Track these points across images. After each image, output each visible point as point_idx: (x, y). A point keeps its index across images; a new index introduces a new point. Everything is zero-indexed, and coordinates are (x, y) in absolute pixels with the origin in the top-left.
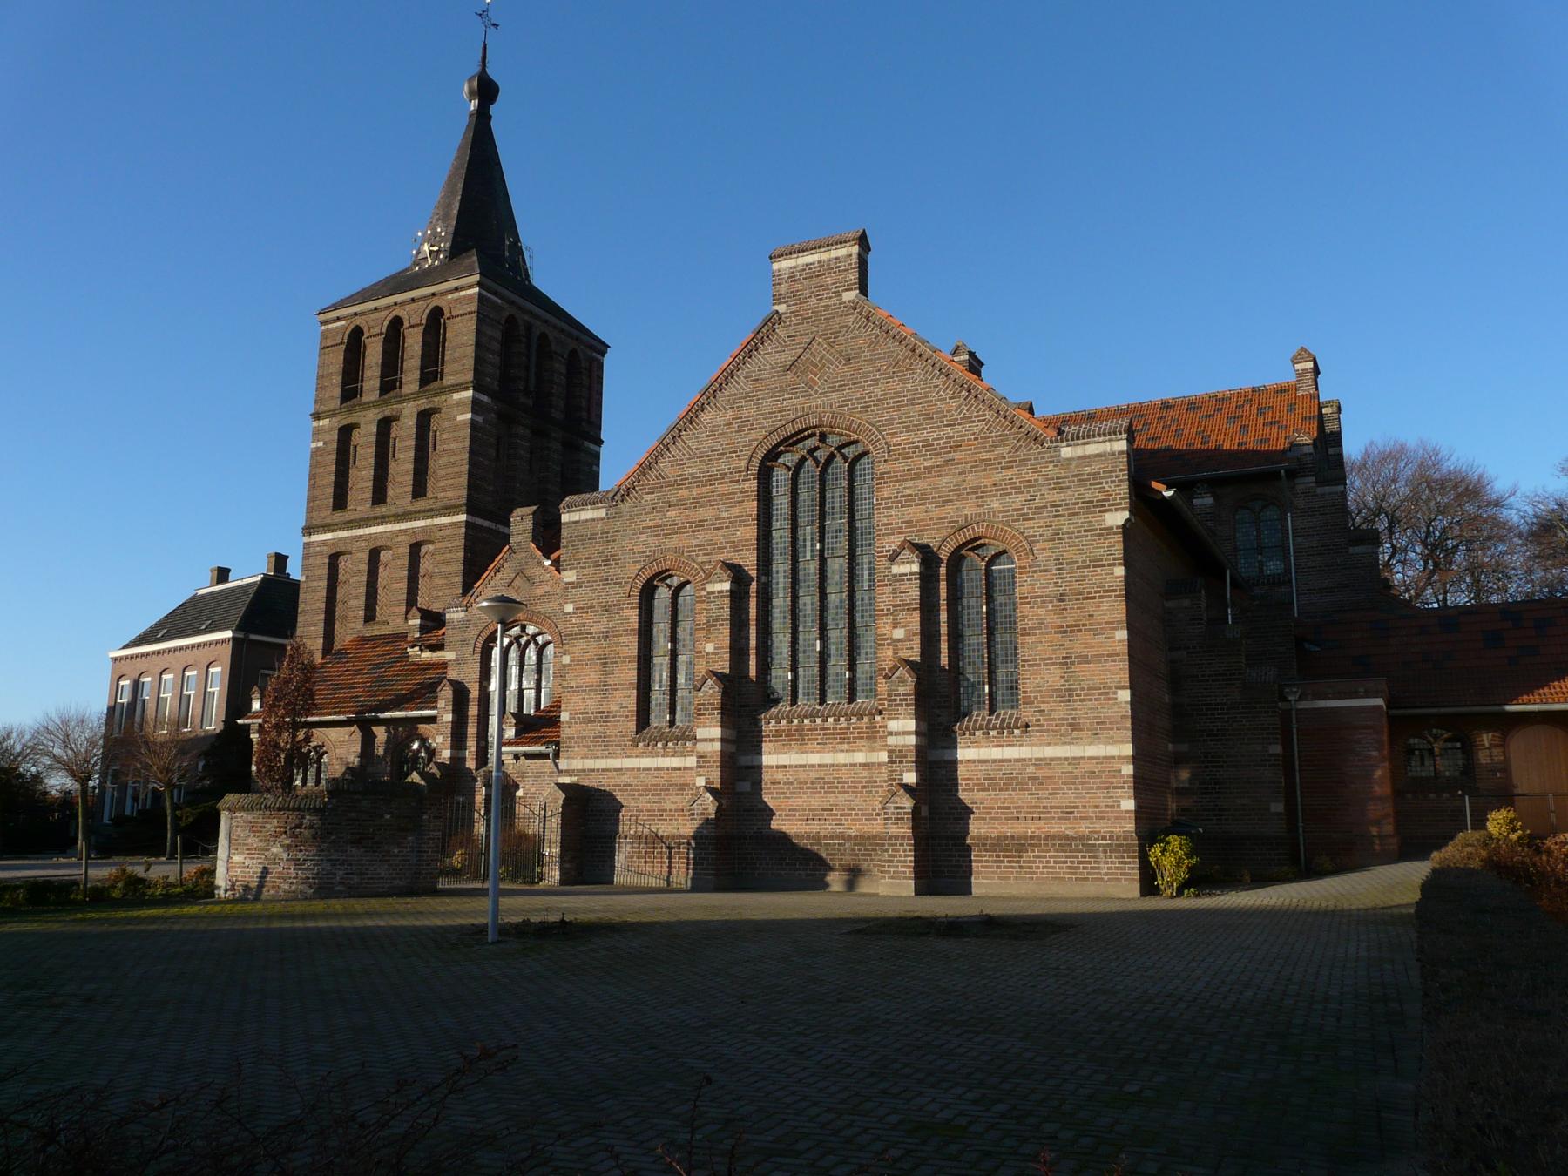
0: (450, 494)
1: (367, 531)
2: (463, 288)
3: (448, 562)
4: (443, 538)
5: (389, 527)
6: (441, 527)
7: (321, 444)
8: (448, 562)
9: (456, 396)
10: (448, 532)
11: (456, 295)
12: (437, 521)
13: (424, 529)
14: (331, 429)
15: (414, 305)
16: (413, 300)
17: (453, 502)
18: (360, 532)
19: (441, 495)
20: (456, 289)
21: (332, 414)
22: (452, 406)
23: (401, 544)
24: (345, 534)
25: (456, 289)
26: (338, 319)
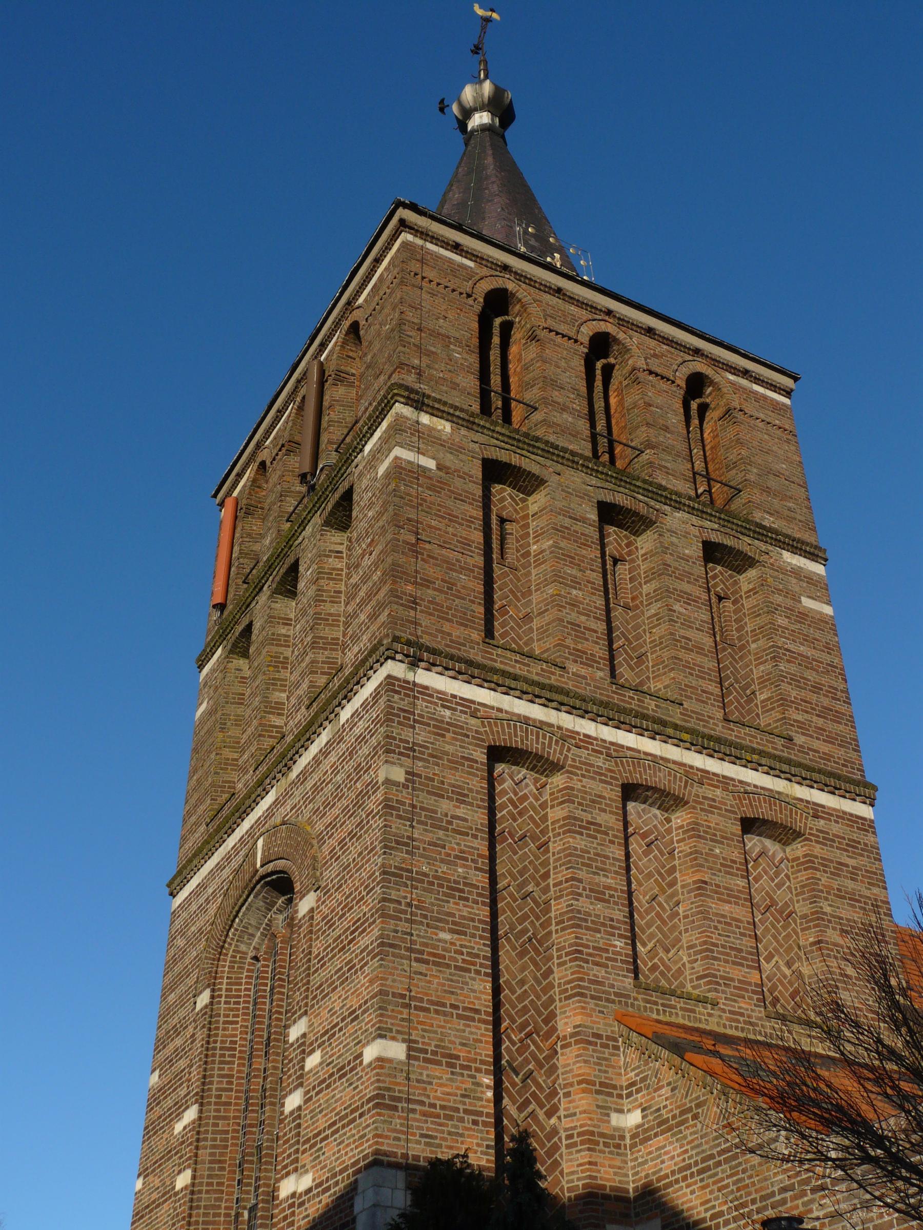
0: (825, 748)
2: (758, 380)
4: (826, 839)
5: (672, 752)
6: (818, 811)
7: (431, 464)
9: (787, 556)
10: (836, 828)
11: (744, 382)
12: (802, 792)
13: (773, 796)
14: (456, 449)
16: (650, 331)
17: (830, 767)
19: (800, 739)
20: (745, 373)
23: (713, 806)
24: (536, 712)
25: (745, 373)
26: (456, 247)
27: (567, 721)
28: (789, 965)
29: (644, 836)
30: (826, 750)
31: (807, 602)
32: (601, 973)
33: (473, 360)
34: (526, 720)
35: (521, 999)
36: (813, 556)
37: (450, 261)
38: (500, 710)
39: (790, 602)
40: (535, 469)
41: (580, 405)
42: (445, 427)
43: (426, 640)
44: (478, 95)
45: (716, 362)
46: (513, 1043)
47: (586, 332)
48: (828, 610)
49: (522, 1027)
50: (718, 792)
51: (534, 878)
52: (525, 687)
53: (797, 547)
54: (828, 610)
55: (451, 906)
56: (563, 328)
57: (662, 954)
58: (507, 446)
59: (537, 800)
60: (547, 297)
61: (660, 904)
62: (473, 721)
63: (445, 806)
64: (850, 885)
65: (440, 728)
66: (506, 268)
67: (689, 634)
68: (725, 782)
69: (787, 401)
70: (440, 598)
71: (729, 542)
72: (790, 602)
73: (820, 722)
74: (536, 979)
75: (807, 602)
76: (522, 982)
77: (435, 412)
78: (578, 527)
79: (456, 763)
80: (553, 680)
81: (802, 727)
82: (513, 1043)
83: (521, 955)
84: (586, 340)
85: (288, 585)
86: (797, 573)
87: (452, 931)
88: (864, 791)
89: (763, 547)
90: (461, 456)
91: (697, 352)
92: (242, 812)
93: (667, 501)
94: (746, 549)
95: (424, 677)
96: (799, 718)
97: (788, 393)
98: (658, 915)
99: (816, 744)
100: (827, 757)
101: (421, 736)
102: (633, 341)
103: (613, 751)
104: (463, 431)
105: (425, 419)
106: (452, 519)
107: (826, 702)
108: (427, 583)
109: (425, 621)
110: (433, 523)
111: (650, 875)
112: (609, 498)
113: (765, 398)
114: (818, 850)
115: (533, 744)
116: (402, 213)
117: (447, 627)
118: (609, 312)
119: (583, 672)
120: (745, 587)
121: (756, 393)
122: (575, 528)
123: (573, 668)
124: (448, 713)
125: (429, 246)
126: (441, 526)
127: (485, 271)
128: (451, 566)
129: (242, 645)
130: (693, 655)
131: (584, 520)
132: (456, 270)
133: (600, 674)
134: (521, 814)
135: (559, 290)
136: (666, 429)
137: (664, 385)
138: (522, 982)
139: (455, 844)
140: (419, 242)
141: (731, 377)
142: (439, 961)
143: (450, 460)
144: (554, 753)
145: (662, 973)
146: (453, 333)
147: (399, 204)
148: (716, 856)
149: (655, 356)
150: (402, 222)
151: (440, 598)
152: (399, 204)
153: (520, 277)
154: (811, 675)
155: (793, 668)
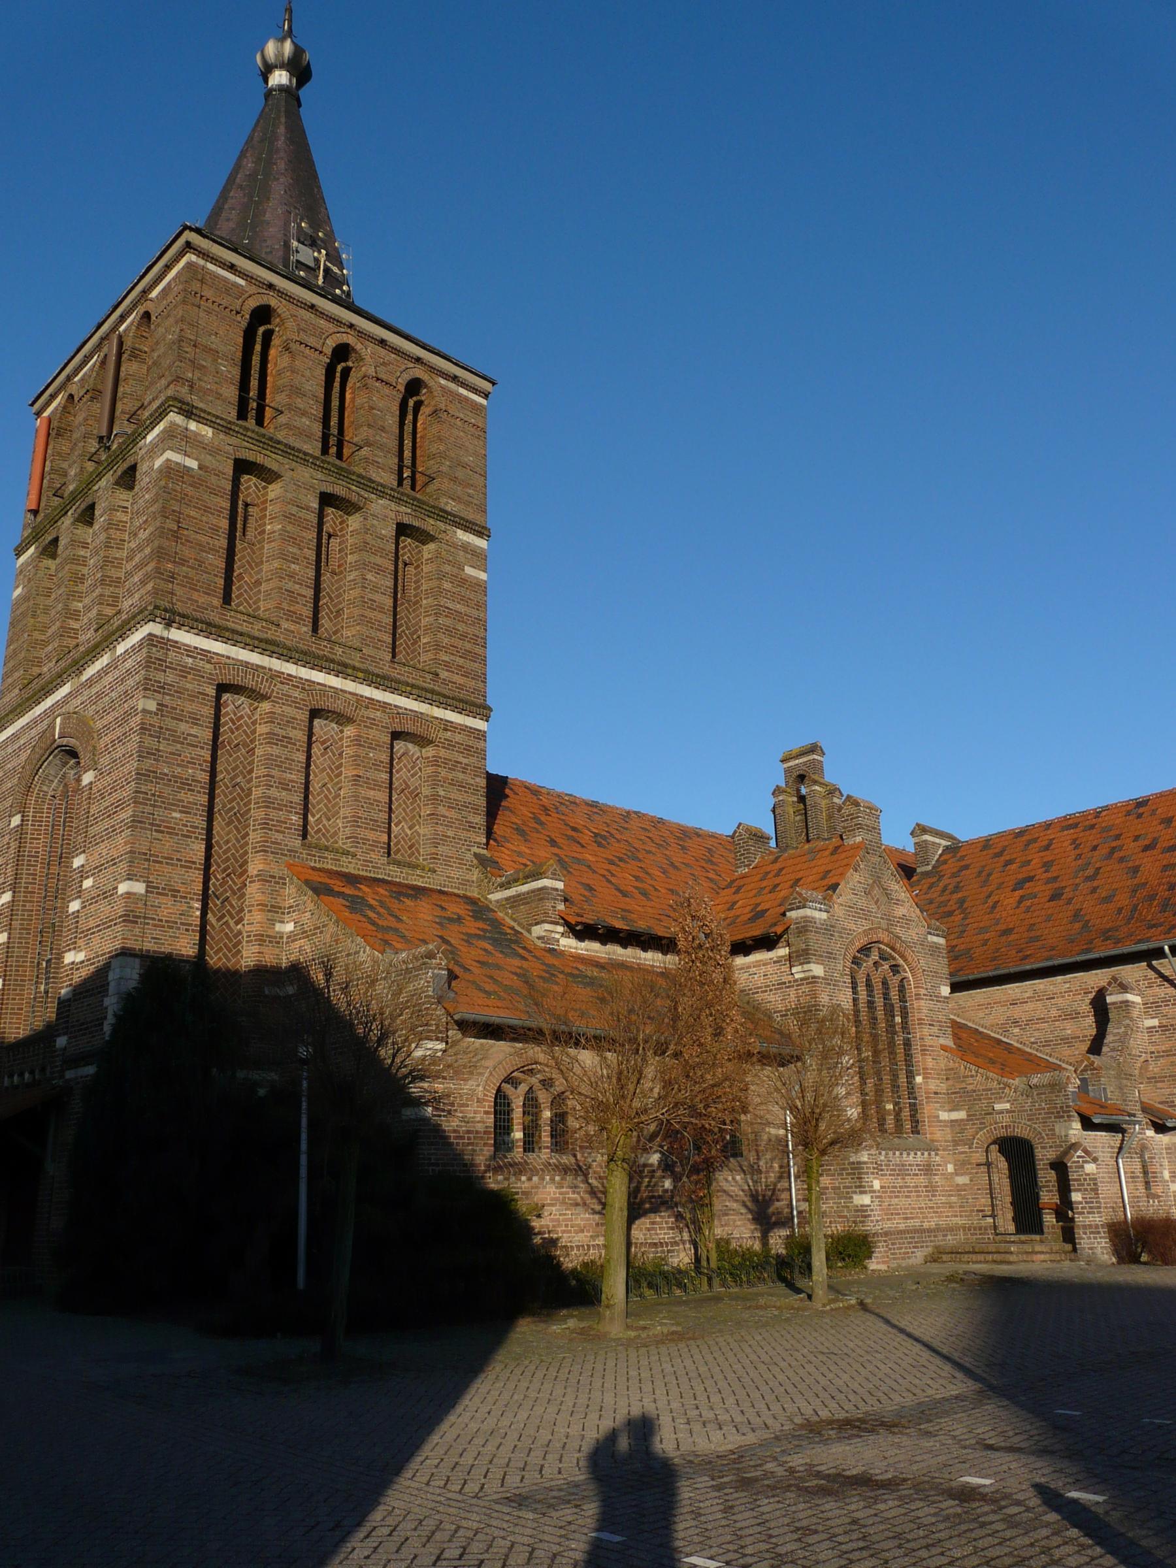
1: (305, 673)
3: (461, 785)
4: (450, 745)
5: (350, 686)
6: (447, 726)
7: (193, 464)
8: (461, 785)
10: (458, 738)
11: (452, 386)
12: (439, 712)
13: (418, 716)
14: (214, 451)
15: (382, 352)
16: (383, 342)
18: (290, 668)
19: (444, 674)
20: (454, 378)
21: (225, 428)
22: (455, 546)
23: (373, 723)
24: (254, 658)
25: (454, 378)
26: (232, 268)
27: (276, 664)
28: (410, 828)
29: (323, 743)
30: (462, 682)
31: (469, 570)
32: (280, 837)
33: (236, 372)
34: (247, 664)
35: (225, 852)
36: (482, 532)
37: (225, 280)
38: (228, 658)
39: (455, 571)
40: (274, 467)
41: (317, 410)
42: (207, 432)
43: (179, 607)
44: (279, 54)
45: (432, 369)
46: (217, 880)
47: (331, 343)
48: (483, 576)
49: (225, 870)
50: (378, 714)
51: (242, 773)
52: (248, 641)
53: (469, 526)
54: (483, 576)
55: (181, 796)
56: (312, 341)
57: (325, 822)
58: (256, 448)
59: (250, 718)
60: (303, 313)
61: (328, 789)
62: (208, 666)
63: (183, 727)
64: (461, 776)
65: (184, 671)
66: (271, 286)
67: (376, 597)
68: (384, 706)
69: (484, 402)
70: (192, 573)
71: (416, 523)
72: (455, 571)
73: (461, 661)
74: (237, 839)
75: (469, 570)
76: (227, 842)
77: (200, 420)
78: (303, 514)
79: (193, 697)
80: (269, 635)
81: (447, 666)
82: (217, 880)
83: (228, 824)
84: (328, 351)
85: (88, 516)
86: (466, 547)
87: (181, 812)
88: (483, 711)
89: (442, 526)
90: (218, 457)
91: (418, 360)
92: (47, 691)
93: (374, 491)
94: (430, 529)
95: (176, 634)
96: (447, 659)
97: (486, 396)
98: (326, 796)
99: (456, 678)
100: (461, 687)
101: (170, 677)
102: (367, 351)
103: (307, 686)
104: (222, 436)
105: (193, 426)
106: (206, 509)
107: (468, 646)
108: (183, 562)
109: (179, 591)
110: (192, 513)
111: (324, 769)
112: (329, 490)
113: (467, 399)
114: (443, 753)
115: (249, 682)
116: (189, 236)
117: (195, 596)
118: (351, 326)
119: (292, 628)
120: (426, 556)
121: (460, 395)
122: (300, 514)
123: (285, 625)
124: (190, 660)
125: (210, 266)
126: (197, 516)
127: (253, 289)
128: (201, 547)
129: (51, 549)
130: (376, 613)
131: (307, 508)
132: (229, 288)
133: (305, 629)
134: (237, 729)
135: (313, 306)
136: (383, 429)
137: (386, 390)
138: (227, 842)
139: (188, 753)
140: (201, 262)
141: (443, 382)
142: (171, 832)
143: (209, 460)
144: (264, 688)
145: (323, 834)
146: (221, 348)
147: (186, 228)
148: (370, 759)
149: (384, 364)
150: (188, 245)
151: (192, 573)
152: (186, 228)
153: (282, 294)
154: (461, 627)
155: (448, 622)
